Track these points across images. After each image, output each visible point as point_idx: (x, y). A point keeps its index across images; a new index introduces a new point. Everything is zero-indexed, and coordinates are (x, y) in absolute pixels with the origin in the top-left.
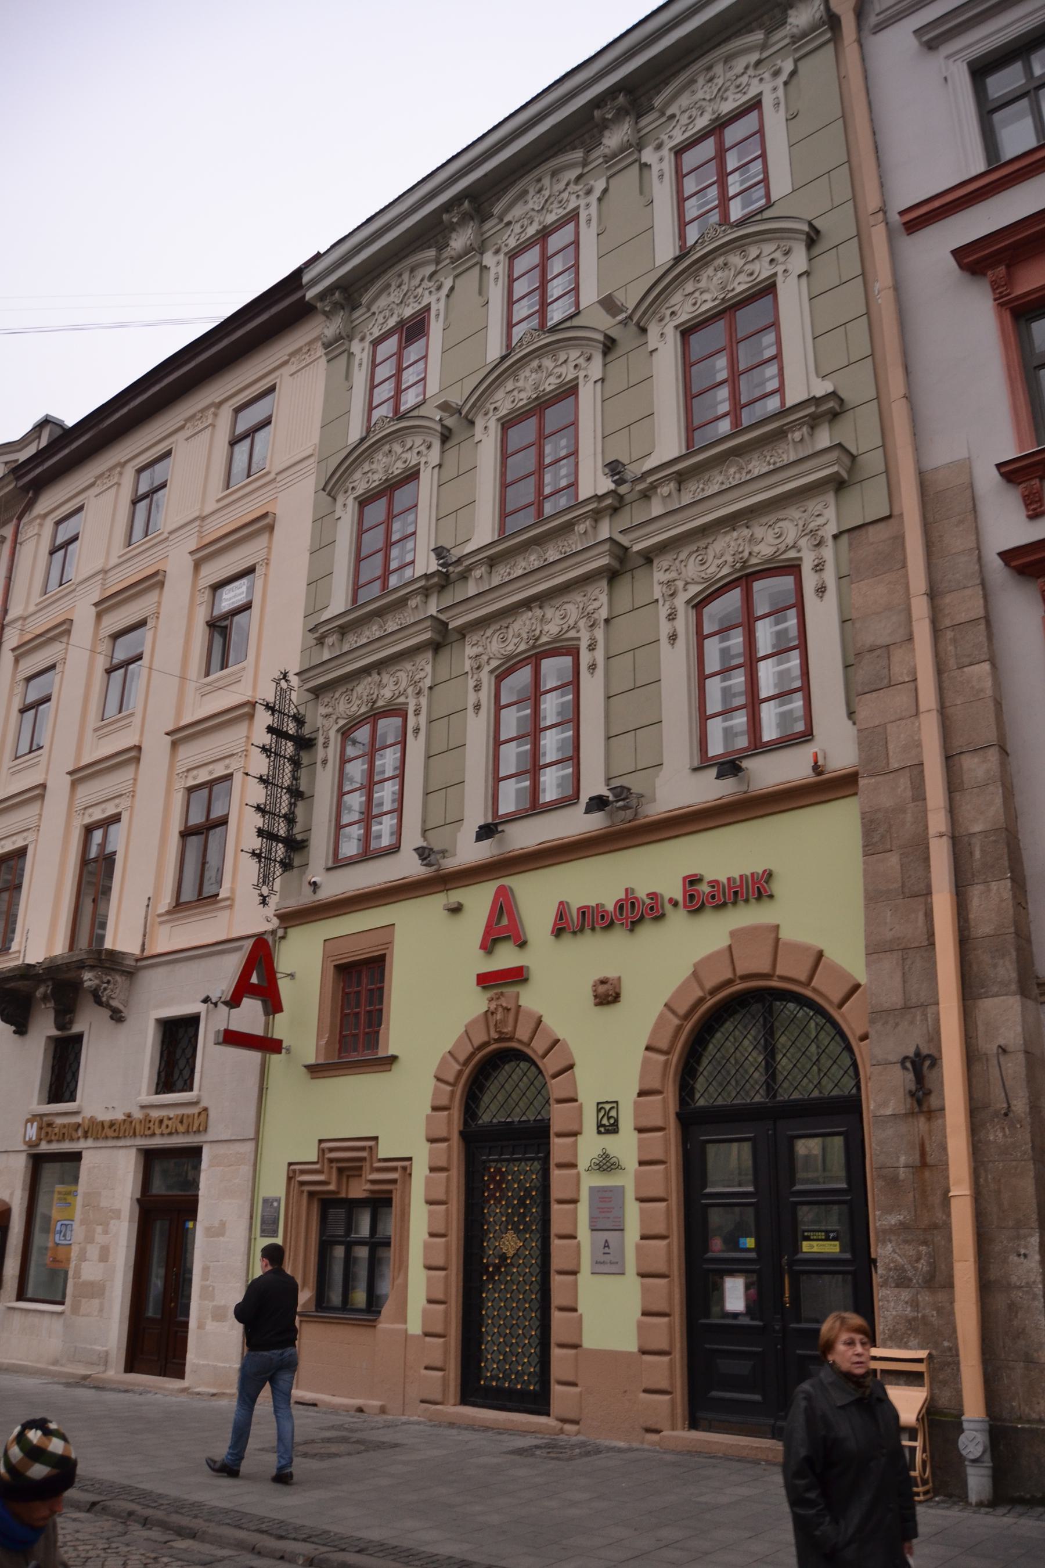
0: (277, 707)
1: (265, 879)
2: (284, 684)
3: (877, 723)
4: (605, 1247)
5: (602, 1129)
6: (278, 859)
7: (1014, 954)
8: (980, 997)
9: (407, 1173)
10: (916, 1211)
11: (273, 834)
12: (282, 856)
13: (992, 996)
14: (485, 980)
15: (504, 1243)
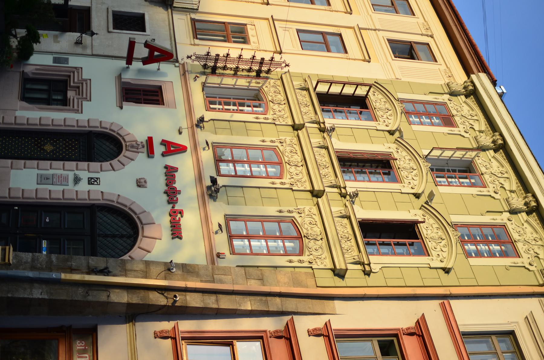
0: (273, 62)
1: (198, 58)
2: (284, 65)
3: (232, 273)
4: (47, 178)
5: (90, 179)
6: (207, 63)
7: (142, 303)
8: (127, 292)
9: (77, 111)
10: (56, 266)
11: (218, 61)
12: (208, 65)
13: (127, 295)
14: (150, 140)
15: (48, 146)
